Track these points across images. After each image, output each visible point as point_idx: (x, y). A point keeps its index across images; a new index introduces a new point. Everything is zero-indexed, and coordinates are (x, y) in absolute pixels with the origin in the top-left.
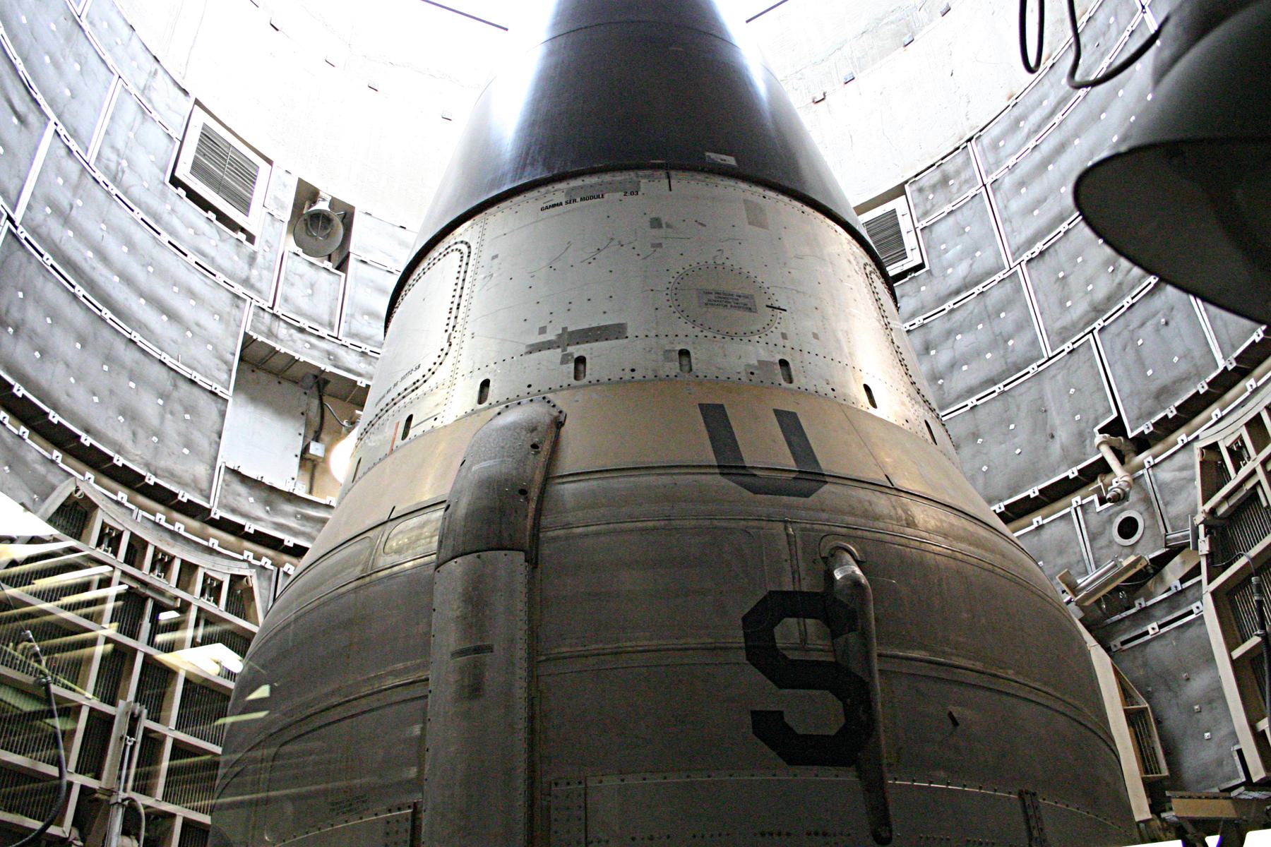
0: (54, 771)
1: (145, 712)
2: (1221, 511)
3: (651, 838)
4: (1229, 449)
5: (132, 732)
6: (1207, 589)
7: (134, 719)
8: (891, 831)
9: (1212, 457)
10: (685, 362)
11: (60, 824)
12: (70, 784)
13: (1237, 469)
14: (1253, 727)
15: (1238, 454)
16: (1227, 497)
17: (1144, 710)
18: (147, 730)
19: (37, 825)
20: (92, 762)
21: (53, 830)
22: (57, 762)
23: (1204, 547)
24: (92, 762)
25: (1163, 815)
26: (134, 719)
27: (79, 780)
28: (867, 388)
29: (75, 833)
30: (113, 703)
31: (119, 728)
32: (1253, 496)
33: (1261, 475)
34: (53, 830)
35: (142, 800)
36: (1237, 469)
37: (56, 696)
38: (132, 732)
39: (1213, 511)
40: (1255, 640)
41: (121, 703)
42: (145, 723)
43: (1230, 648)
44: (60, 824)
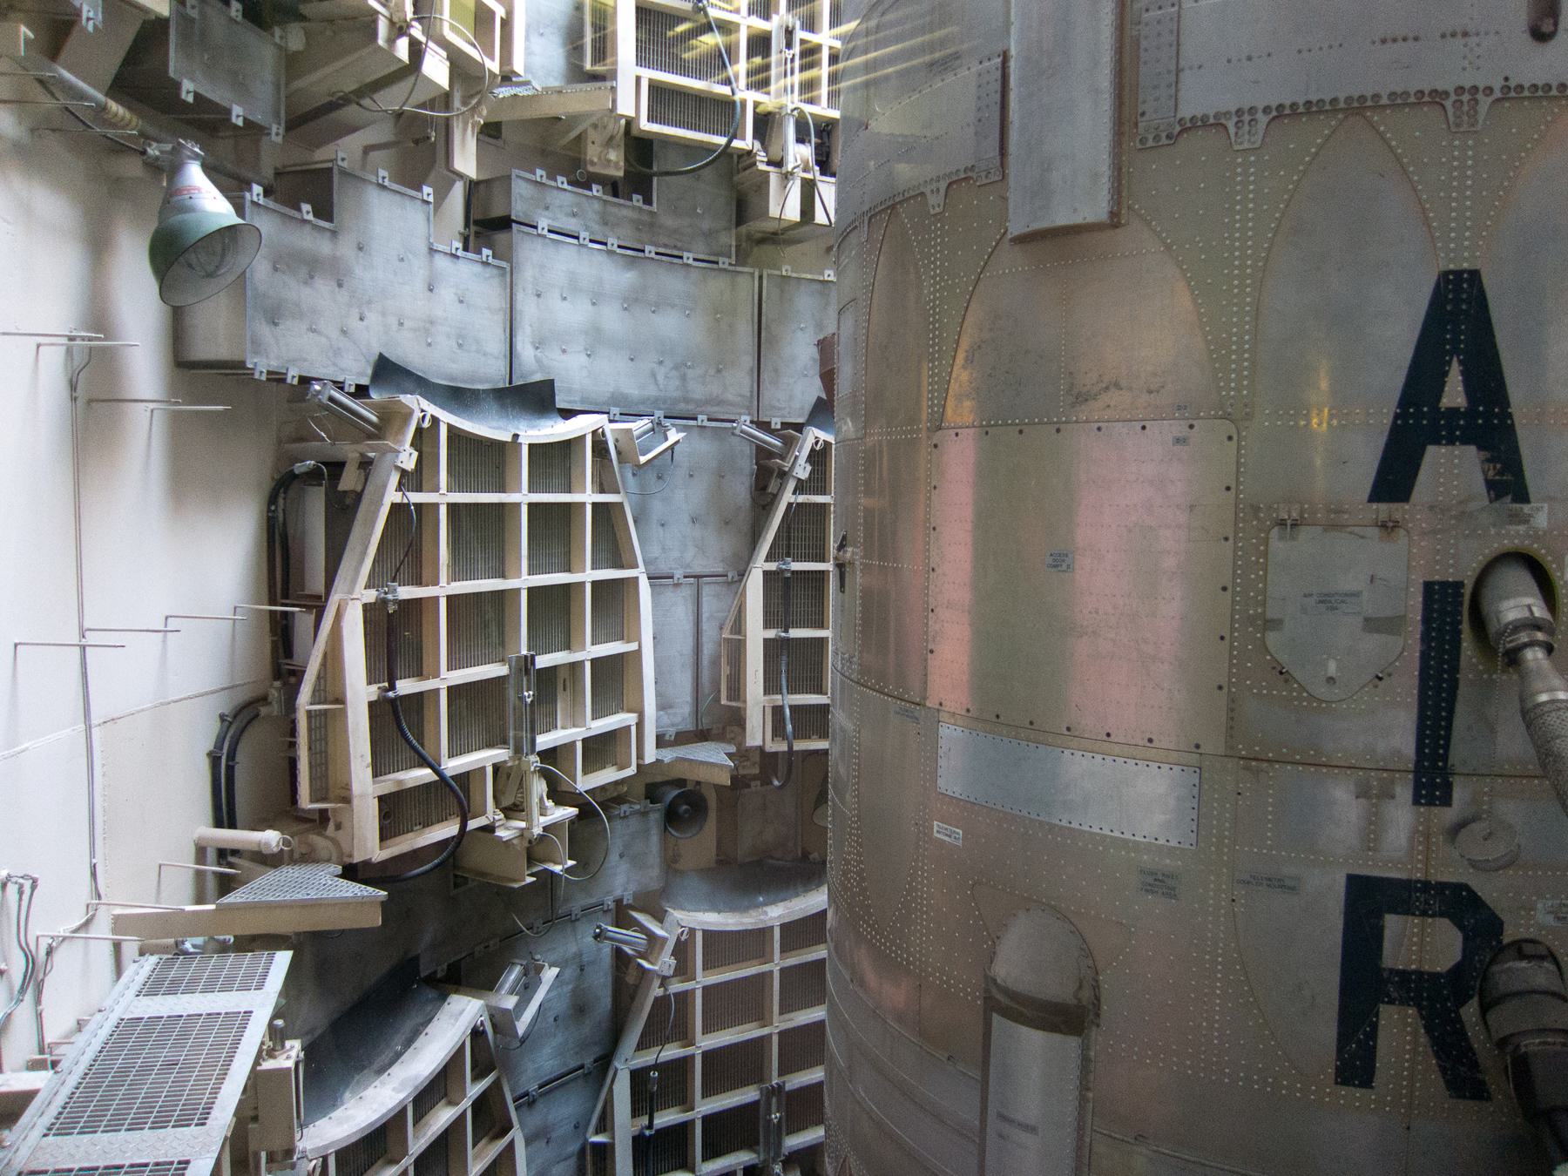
0: (726, 90)
1: (798, 24)
3: (1249, 58)
5: (789, 45)
7: (789, 33)
8: (1556, 24)
11: (743, 139)
12: (744, 103)
18: (803, 42)
19: (721, 141)
20: (760, 80)
21: (736, 144)
22: (727, 82)
24: (760, 80)
26: (789, 33)
27: (751, 97)
29: (757, 145)
30: (767, 17)
31: (777, 42)
34: (736, 144)
35: (808, 109)
37: (717, 20)
38: (789, 45)
41: (775, 18)
42: (800, 34)
44: (743, 139)
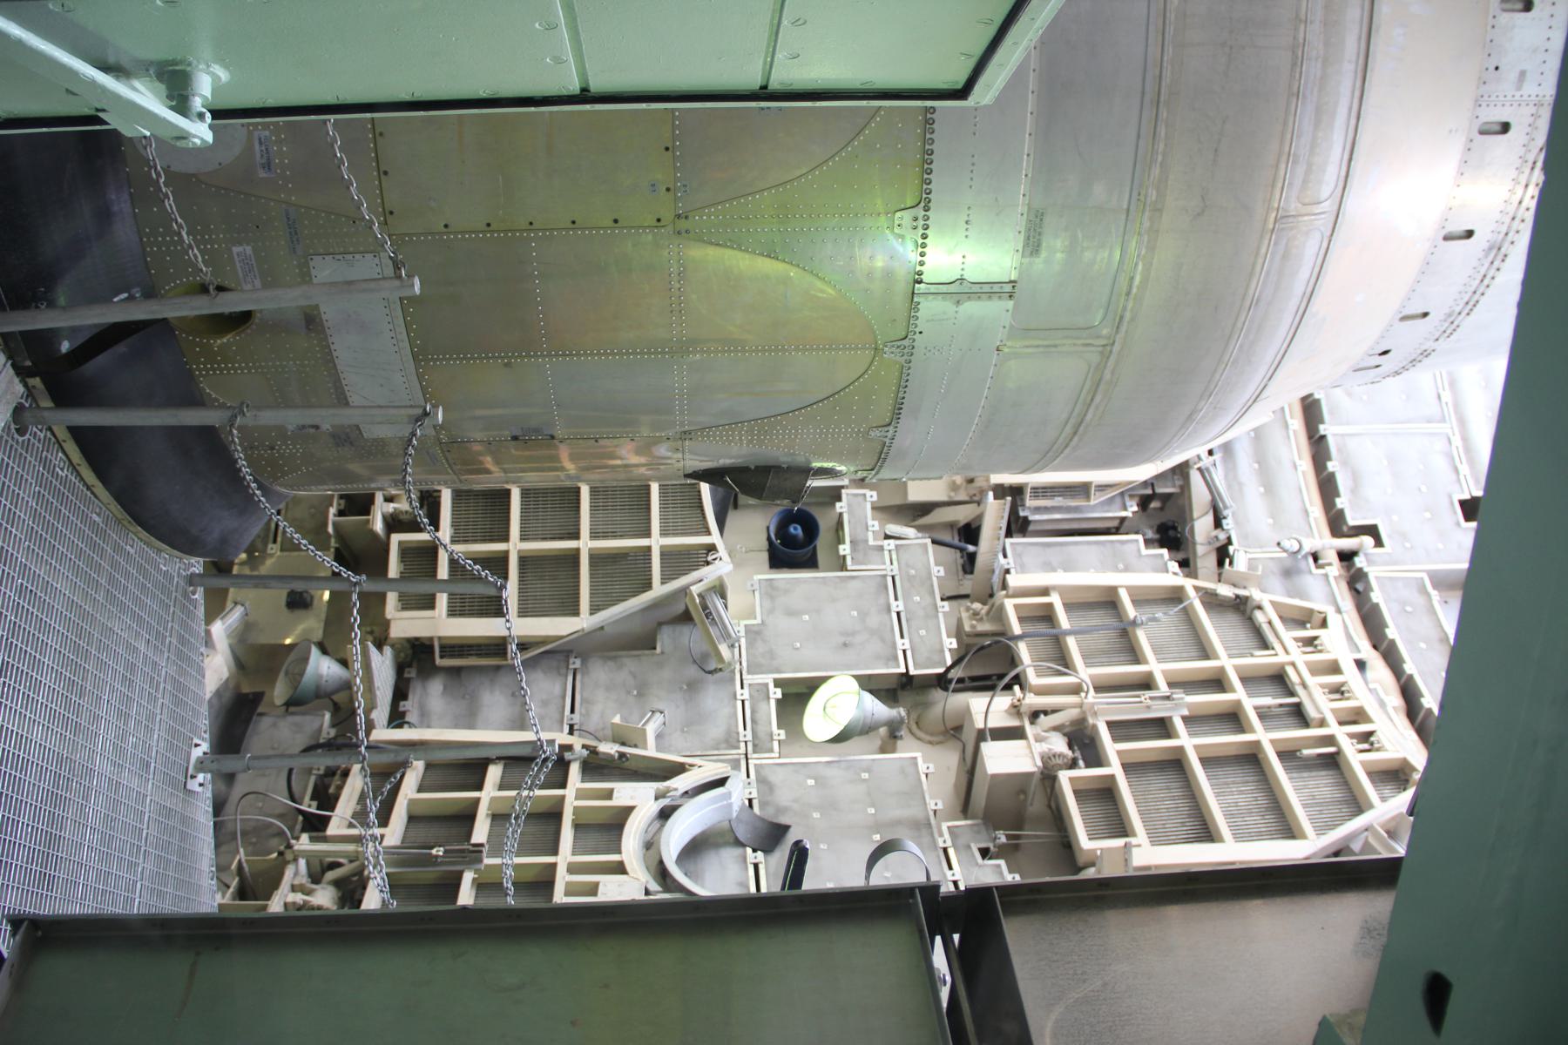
2: (1259, 617)
4: (1316, 638)
6: (1188, 584)
9: (1317, 619)
10: (1498, 128)
13: (1297, 640)
14: (1054, 588)
15: (1310, 642)
16: (1270, 623)
17: (1088, 497)
23: (1225, 591)
25: (991, 494)
28: (1425, 315)
32: (1265, 645)
33: (1282, 658)
36: (1297, 640)
39: (1260, 608)
40: (1131, 612)
43: (1129, 588)
